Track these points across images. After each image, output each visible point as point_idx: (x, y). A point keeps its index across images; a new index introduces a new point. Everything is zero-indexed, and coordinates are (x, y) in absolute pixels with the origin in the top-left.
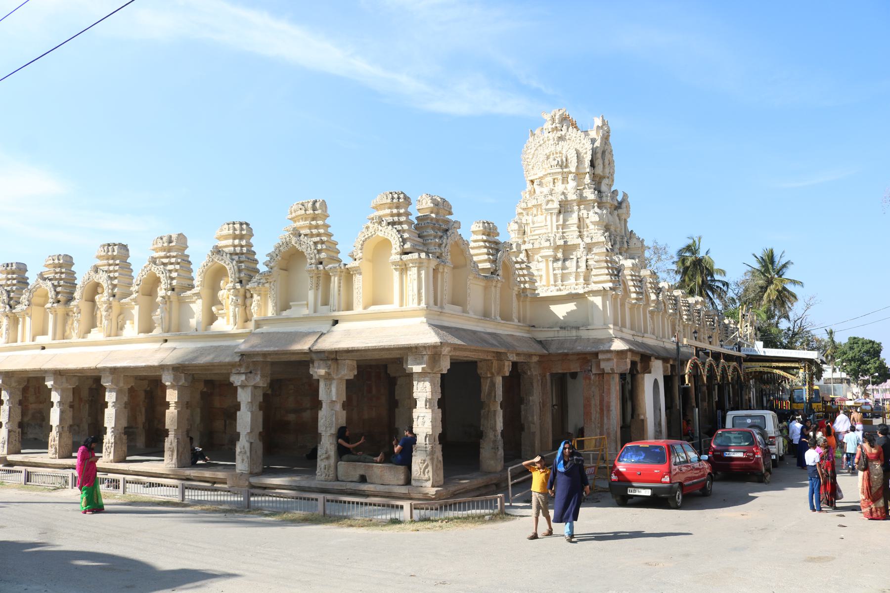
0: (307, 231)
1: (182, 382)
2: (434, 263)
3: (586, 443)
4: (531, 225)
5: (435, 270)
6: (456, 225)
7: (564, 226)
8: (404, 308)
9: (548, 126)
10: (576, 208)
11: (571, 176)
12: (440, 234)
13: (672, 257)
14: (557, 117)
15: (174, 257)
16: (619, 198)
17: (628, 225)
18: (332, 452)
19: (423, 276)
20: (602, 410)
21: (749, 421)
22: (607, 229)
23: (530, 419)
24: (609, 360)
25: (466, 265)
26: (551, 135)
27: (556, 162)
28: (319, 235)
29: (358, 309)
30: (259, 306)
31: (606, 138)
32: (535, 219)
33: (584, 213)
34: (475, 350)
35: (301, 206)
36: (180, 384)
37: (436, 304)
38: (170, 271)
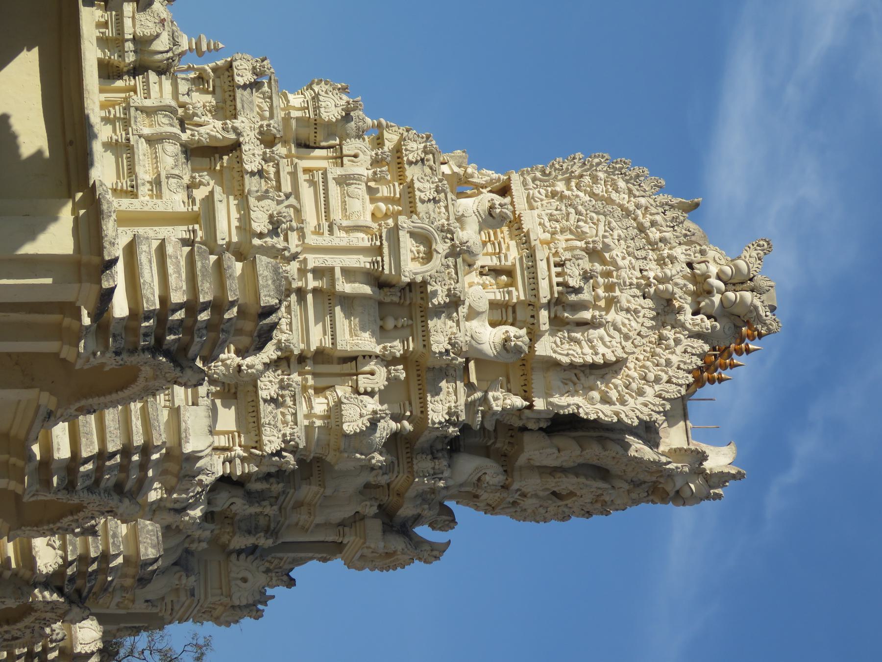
7: (328, 299)
9: (715, 265)
10: (397, 347)
16: (423, 531)
17: (313, 566)
27: (572, 282)
31: (658, 486)
32: (360, 190)
33: (377, 377)
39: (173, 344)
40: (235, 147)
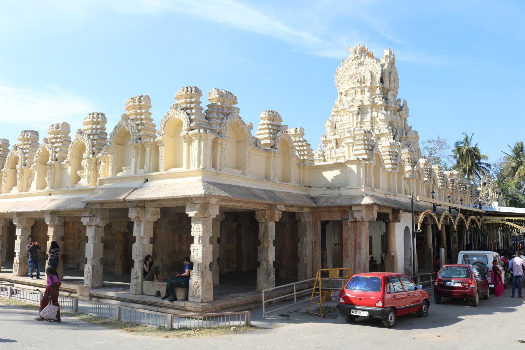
0: (133, 117)
1: (57, 222)
2: (211, 137)
3: (331, 273)
4: (340, 123)
5: (215, 143)
6: (236, 111)
7: (361, 122)
8: (191, 169)
9: (352, 56)
10: (369, 110)
11: (366, 89)
12: (221, 116)
13: (449, 147)
14: (358, 50)
15: (59, 138)
18: (140, 274)
19: (202, 146)
20: (355, 248)
21: (475, 259)
22: (391, 124)
23: (304, 254)
24: (359, 211)
25: (245, 140)
26: (354, 62)
27: (357, 80)
28: (142, 119)
29: (162, 171)
30: (104, 170)
31: (392, 63)
33: (375, 114)
34: (248, 202)
35: (131, 100)
36: (55, 224)
37: (214, 166)
38: (56, 147)
39: (371, 148)
40: (336, 139)
